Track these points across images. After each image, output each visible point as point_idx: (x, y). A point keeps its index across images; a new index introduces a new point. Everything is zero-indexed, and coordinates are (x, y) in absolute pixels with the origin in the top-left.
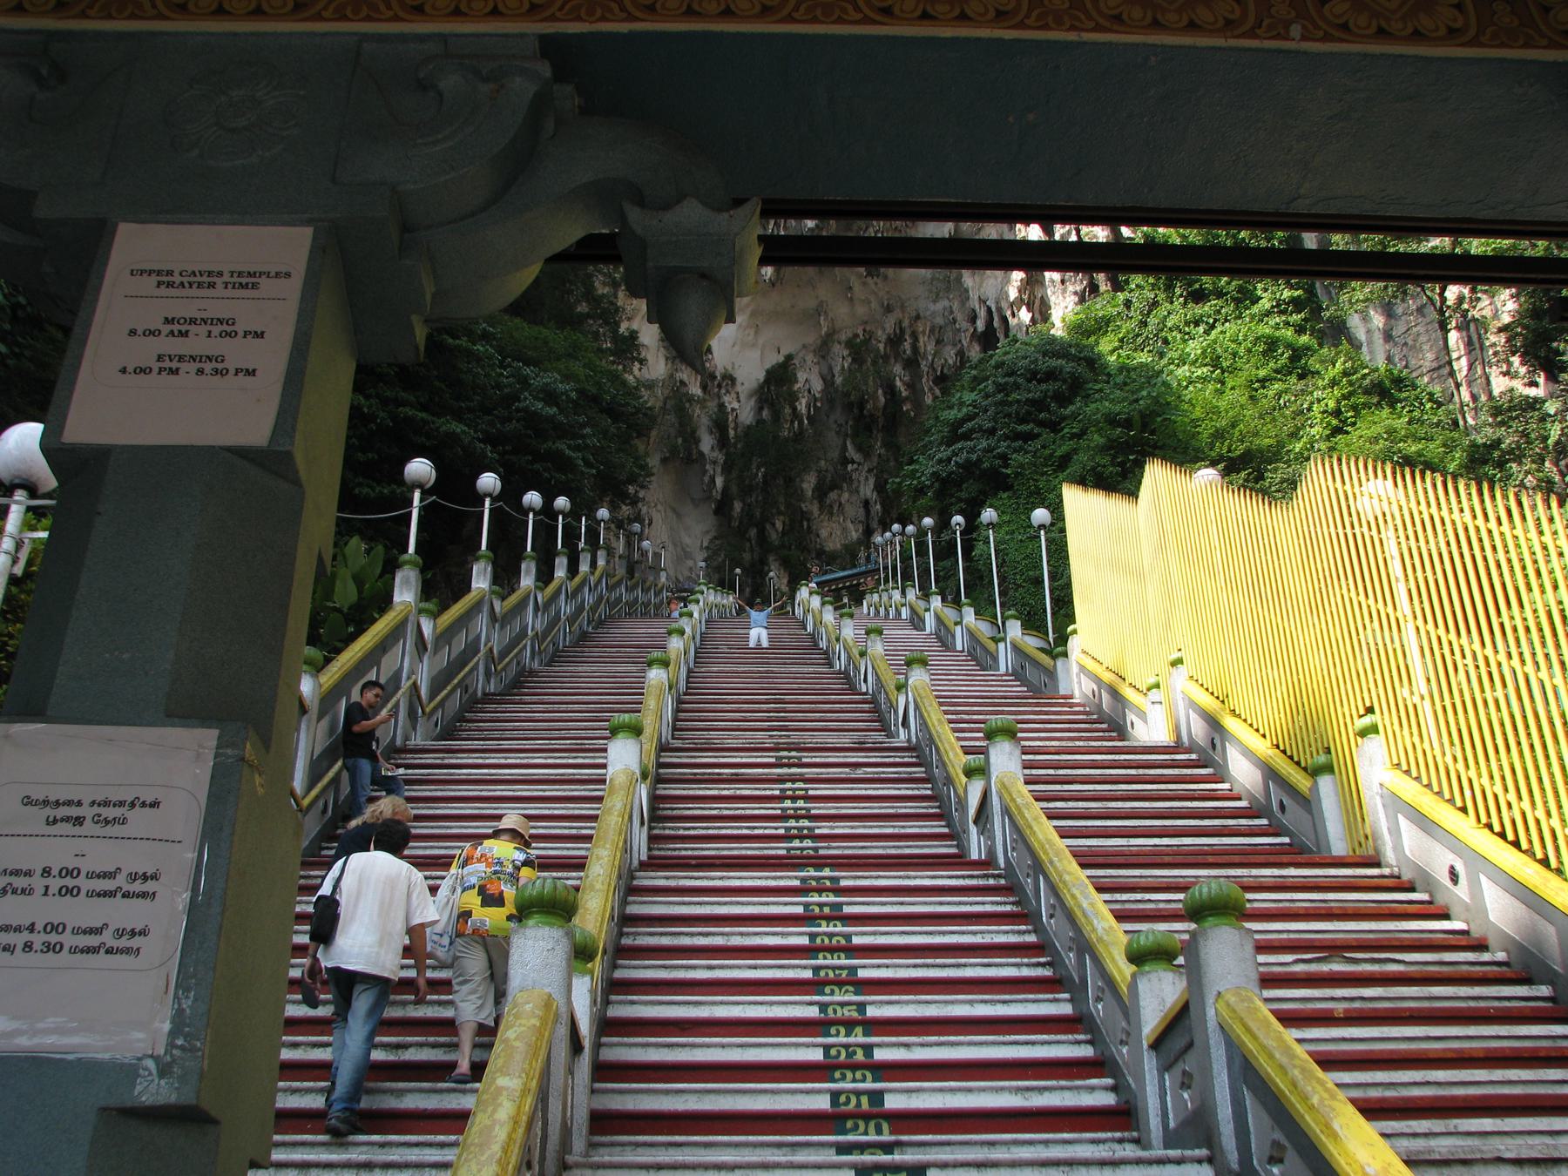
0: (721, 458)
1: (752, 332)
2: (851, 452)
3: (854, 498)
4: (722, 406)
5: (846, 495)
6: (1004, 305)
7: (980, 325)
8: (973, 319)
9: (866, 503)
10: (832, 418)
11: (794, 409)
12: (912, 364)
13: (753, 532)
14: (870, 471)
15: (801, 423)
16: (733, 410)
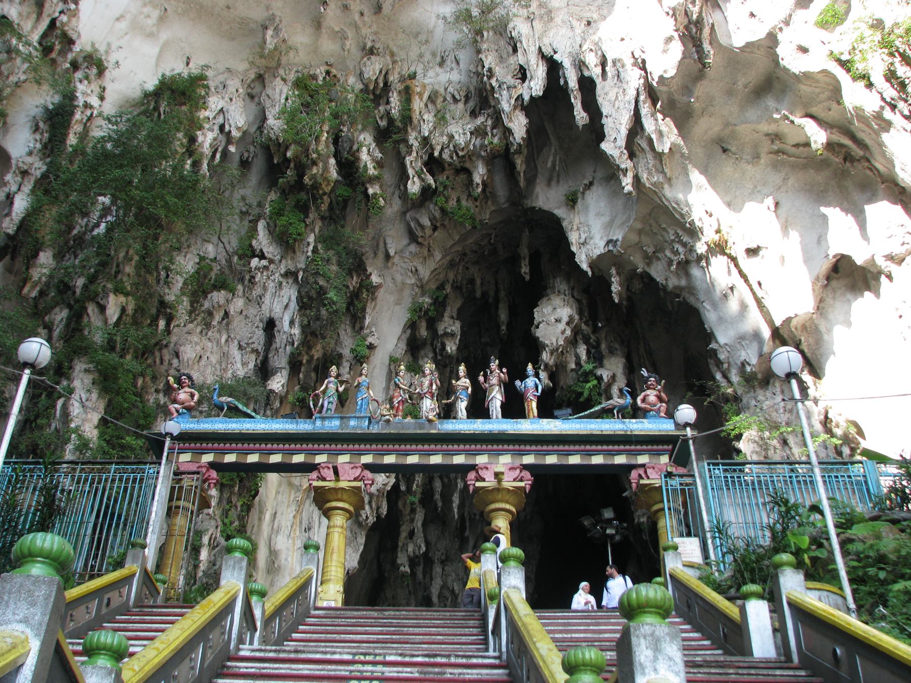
0: (38, 167)
1: (156, 14)
2: (263, 240)
3: (252, 311)
4: (70, 97)
5: (239, 303)
6: (592, 60)
7: (537, 85)
8: (523, 74)
9: (270, 326)
10: (237, 195)
11: (193, 140)
12: (391, 135)
13: (60, 316)
14: (288, 274)
15: (196, 164)
16: (87, 106)
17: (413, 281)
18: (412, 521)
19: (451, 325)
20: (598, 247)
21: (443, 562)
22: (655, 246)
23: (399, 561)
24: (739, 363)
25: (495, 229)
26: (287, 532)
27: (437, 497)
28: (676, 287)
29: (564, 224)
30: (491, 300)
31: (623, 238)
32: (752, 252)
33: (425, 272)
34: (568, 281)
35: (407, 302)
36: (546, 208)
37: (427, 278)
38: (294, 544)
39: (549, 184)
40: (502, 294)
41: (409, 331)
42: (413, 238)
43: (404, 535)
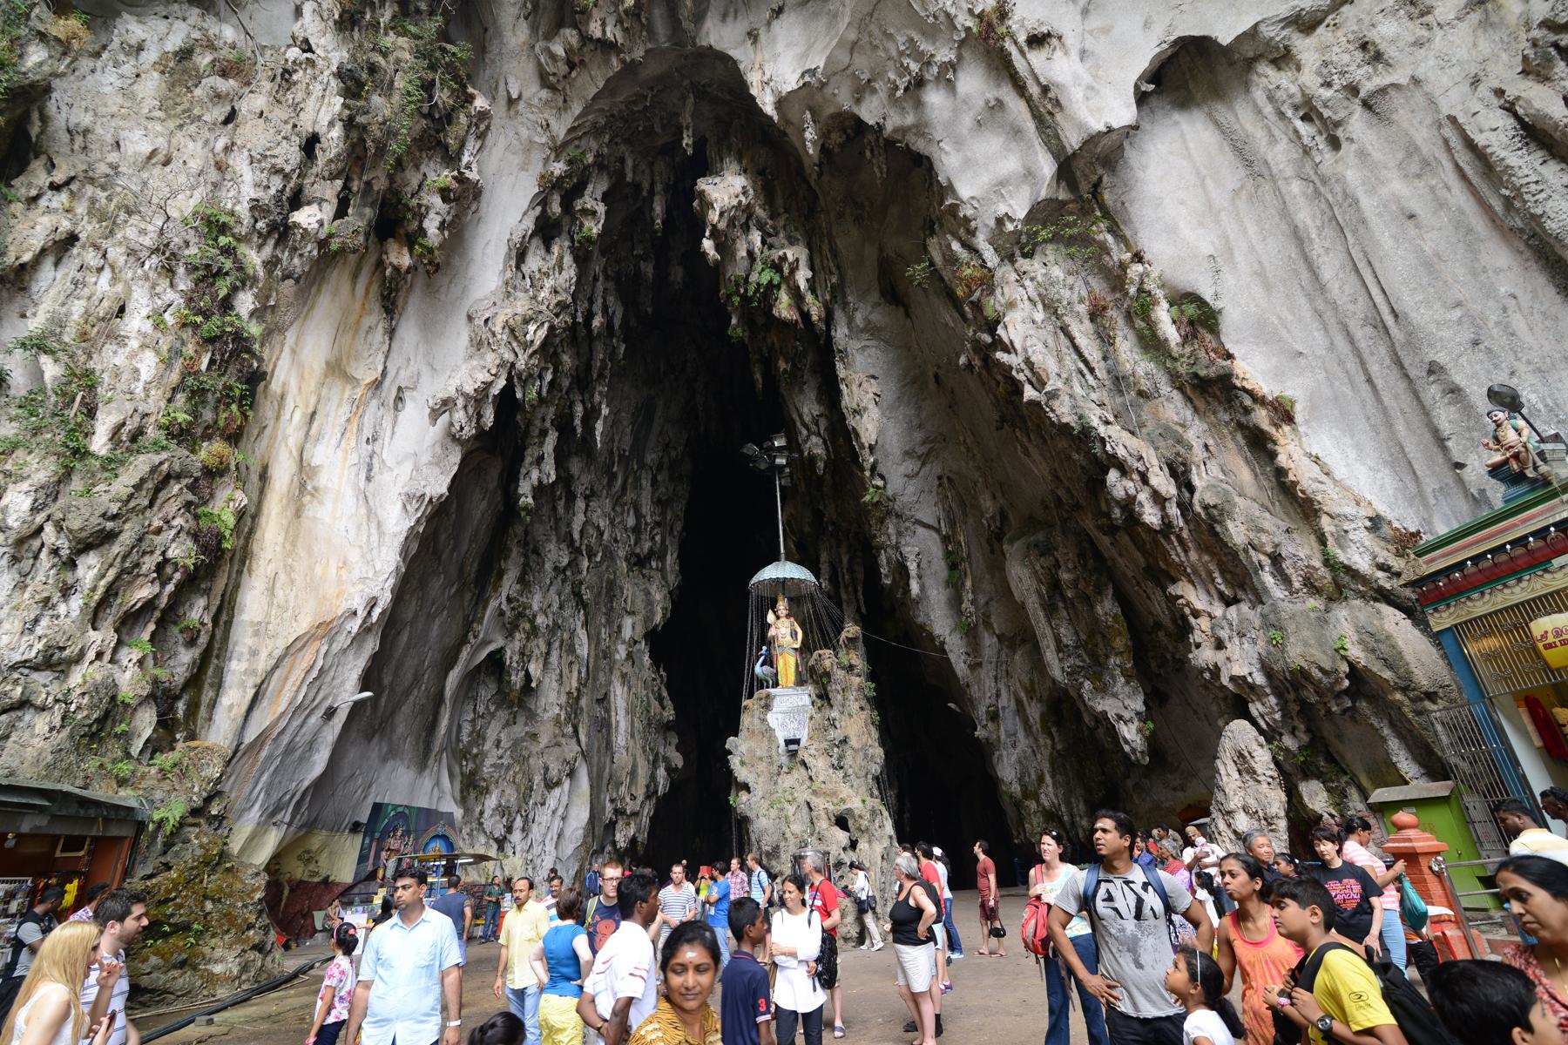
17: (544, 140)
18: (542, 444)
19: (592, 199)
20: (790, 81)
21: (587, 498)
22: (872, 70)
23: (521, 491)
24: (992, 223)
25: (652, 89)
26: (334, 442)
27: (577, 422)
28: (896, 130)
29: (741, 67)
30: (645, 193)
31: (826, 64)
32: (1038, 41)
33: (560, 129)
34: (740, 162)
35: (537, 168)
36: (718, 46)
37: (561, 136)
38: (345, 459)
39: (724, 17)
40: (659, 187)
41: (539, 209)
42: (544, 79)
43: (528, 460)
